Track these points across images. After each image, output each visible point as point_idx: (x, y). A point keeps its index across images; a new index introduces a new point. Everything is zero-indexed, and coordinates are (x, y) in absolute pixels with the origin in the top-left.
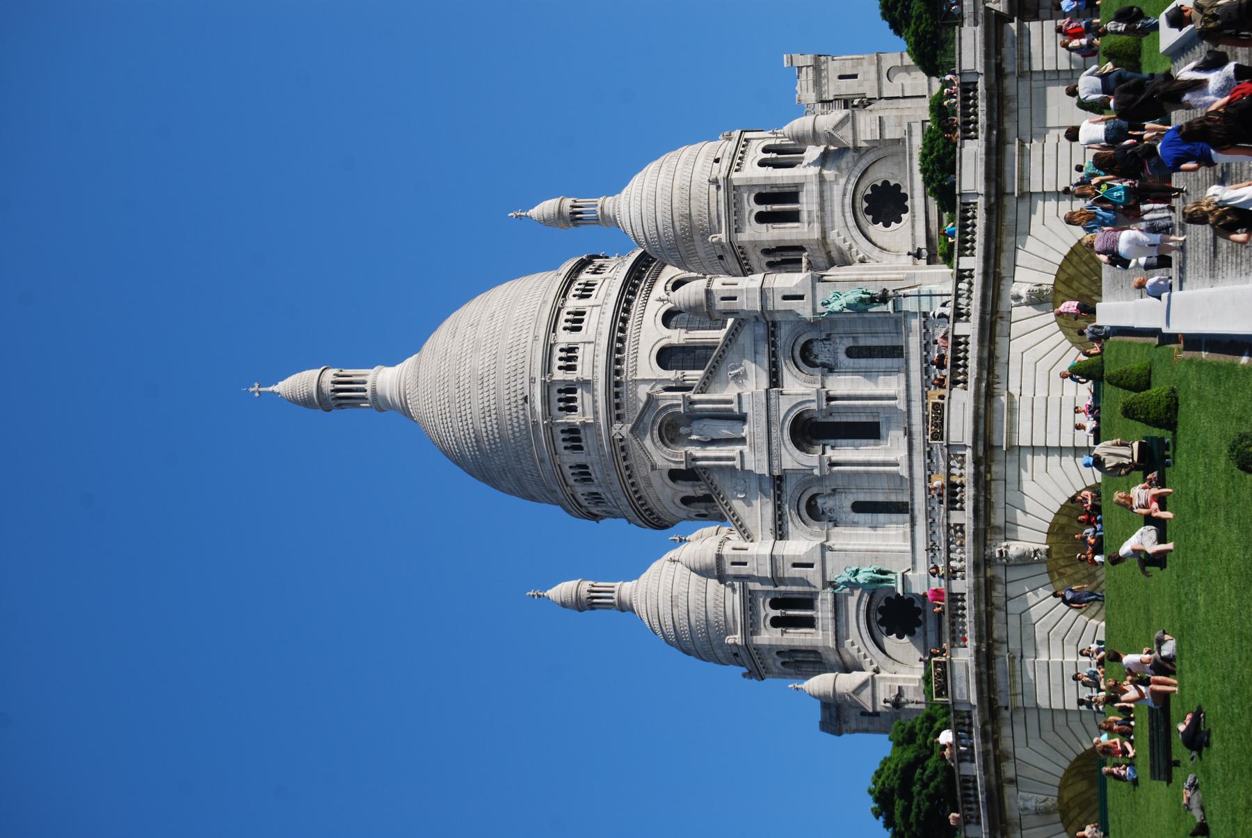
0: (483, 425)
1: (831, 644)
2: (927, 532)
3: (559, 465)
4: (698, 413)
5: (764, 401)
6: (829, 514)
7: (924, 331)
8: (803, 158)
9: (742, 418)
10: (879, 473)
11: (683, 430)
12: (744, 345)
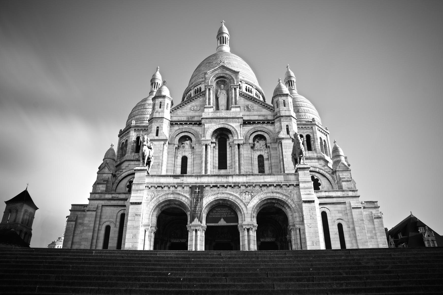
0: (214, 63)
1: (128, 159)
2: (169, 184)
3: (201, 83)
4: (230, 92)
5: (237, 116)
6: (182, 146)
7: (288, 184)
8: (324, 154)
9: (228, 108)
10: (201, 168)
11: (222, 86)
12: (262, 111)
